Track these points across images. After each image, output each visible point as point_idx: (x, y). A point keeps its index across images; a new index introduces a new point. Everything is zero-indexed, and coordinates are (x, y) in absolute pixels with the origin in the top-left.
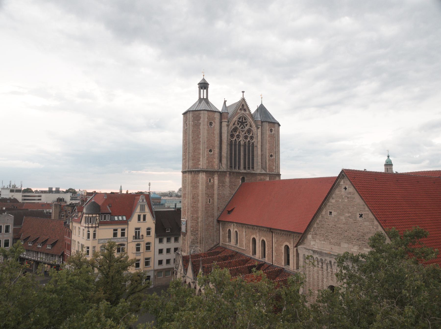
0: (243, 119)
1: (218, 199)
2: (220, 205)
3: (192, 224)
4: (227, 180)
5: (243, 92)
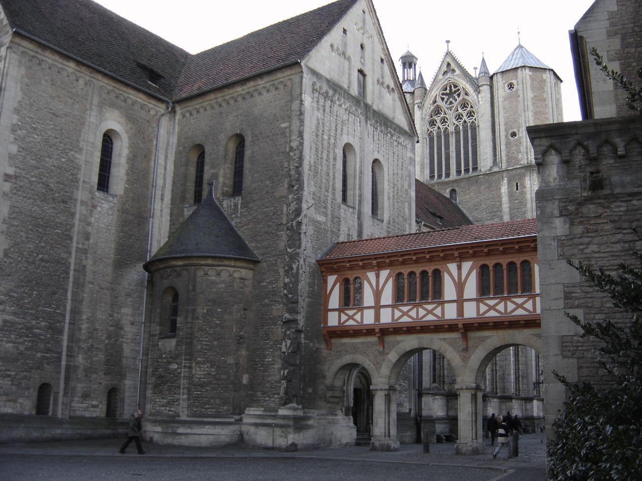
5: (448, 42)
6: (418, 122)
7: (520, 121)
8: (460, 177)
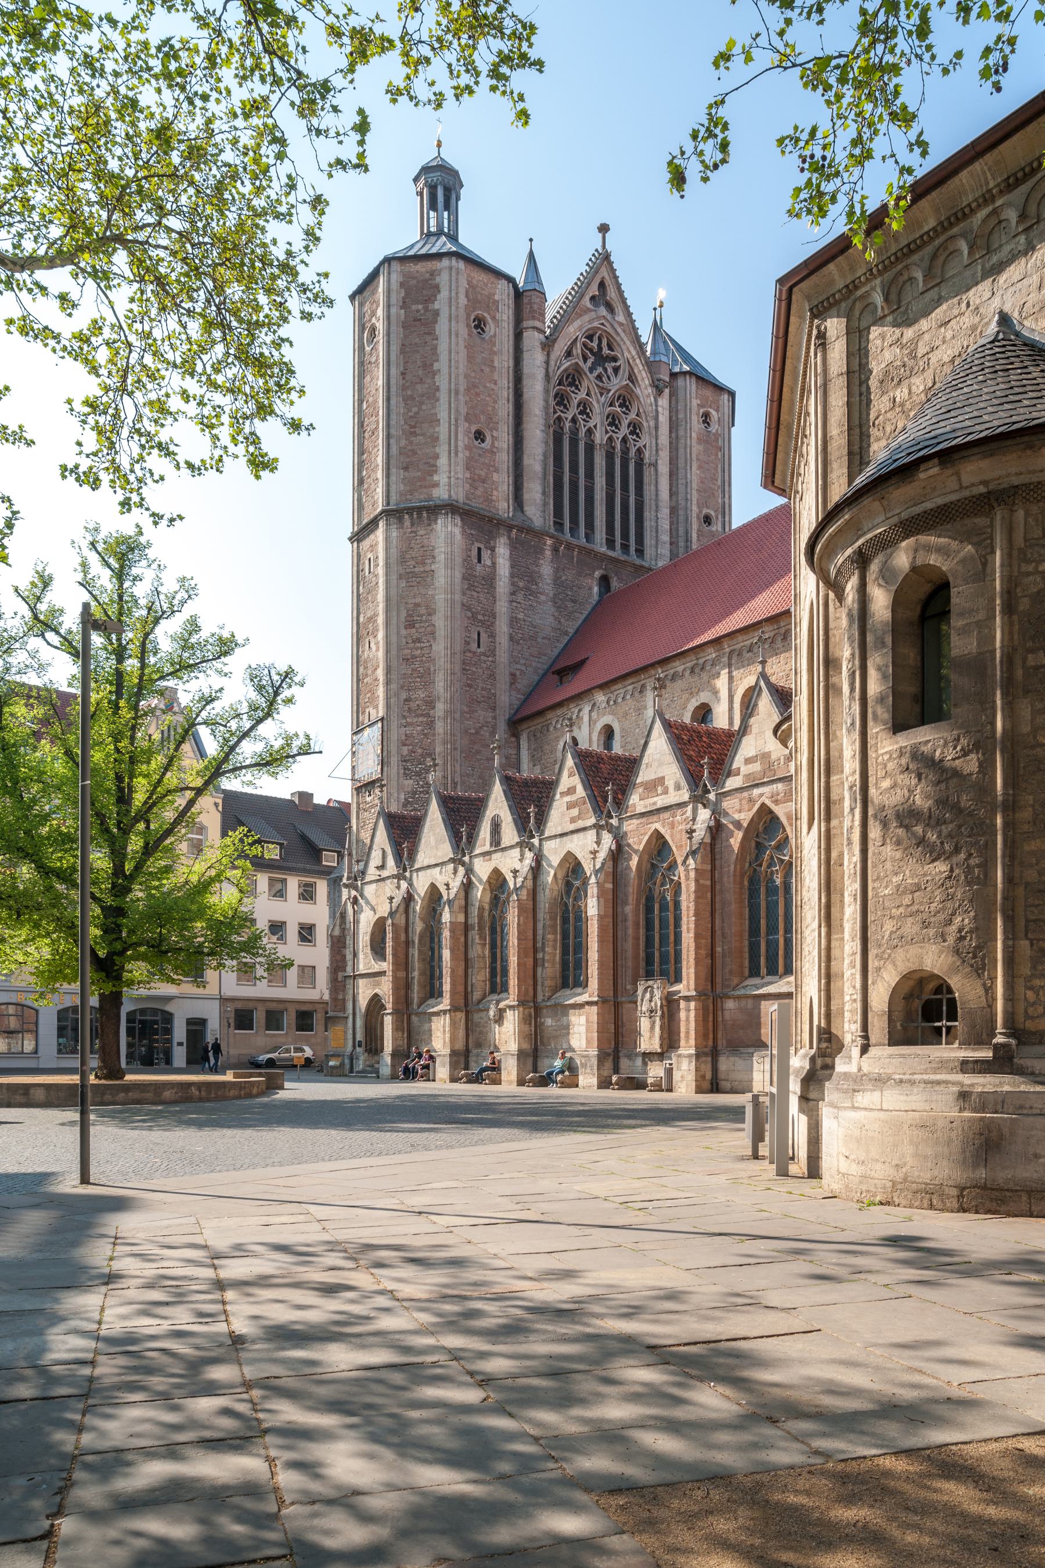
0: (604, 342)
1: (511, 638)
2: (518, 666)
3: (408, 730)
4: (546, 569)
5: (604, 229)
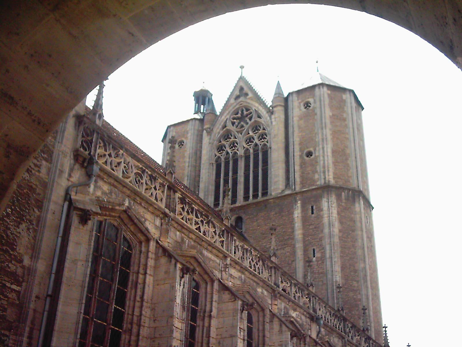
5: (242, 67)
6: (206, 147)
7: (317, 140)
8: (247, 202)
